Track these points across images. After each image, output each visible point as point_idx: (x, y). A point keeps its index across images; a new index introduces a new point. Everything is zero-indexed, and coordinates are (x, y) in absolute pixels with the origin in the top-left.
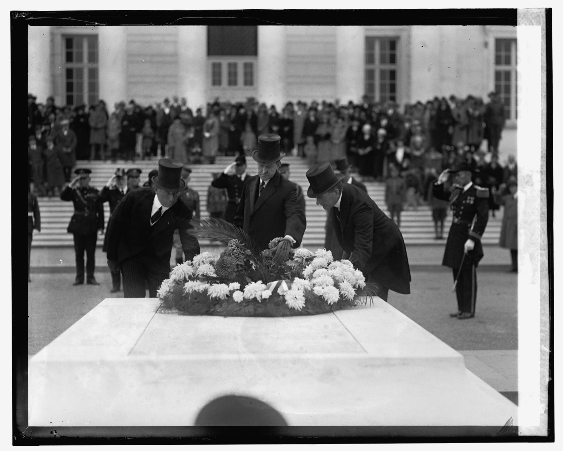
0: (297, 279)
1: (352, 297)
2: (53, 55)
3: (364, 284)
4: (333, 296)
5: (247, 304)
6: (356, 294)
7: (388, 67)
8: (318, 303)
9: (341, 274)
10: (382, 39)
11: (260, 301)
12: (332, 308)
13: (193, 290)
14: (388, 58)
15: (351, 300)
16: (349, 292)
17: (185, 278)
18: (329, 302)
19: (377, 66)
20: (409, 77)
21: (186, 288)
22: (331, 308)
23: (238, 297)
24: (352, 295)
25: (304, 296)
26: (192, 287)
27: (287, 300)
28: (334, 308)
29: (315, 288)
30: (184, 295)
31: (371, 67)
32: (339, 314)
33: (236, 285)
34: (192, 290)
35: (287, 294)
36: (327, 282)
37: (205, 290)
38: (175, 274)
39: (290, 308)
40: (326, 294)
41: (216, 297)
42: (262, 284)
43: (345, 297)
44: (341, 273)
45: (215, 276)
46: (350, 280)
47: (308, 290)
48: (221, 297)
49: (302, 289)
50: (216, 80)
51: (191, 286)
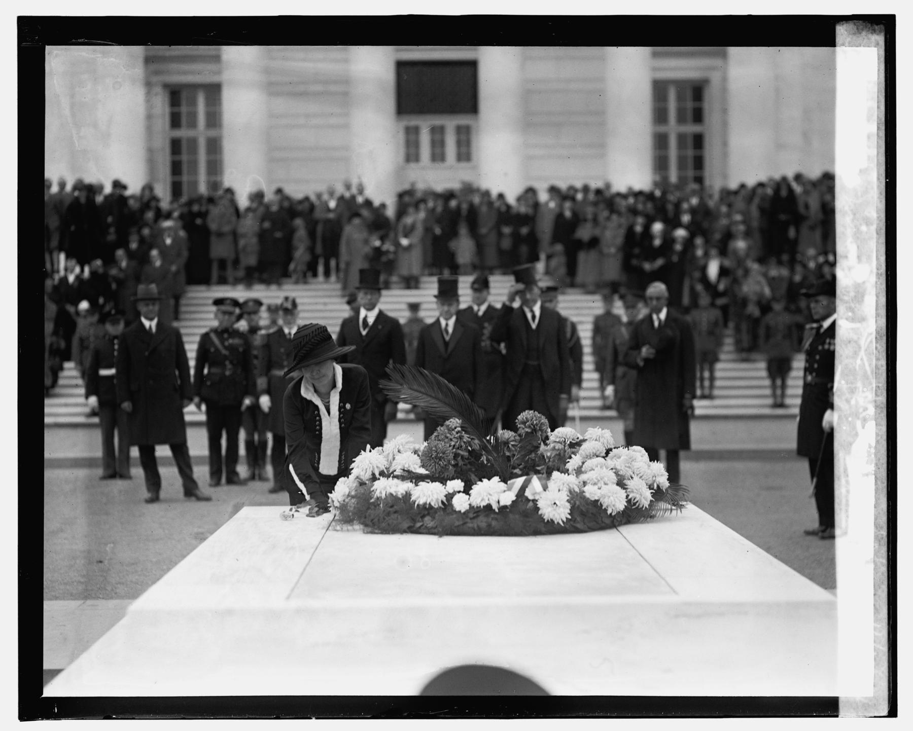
0: (556, 474)
1: (646, 503)
2: (149, 117)
3: (667, 484)
4: (615, 501)
5: (475, 515)
6: (654, 500)
7: (691, 129)
8: (592, 514)
9: (629, 467)
10: (680, 84)
11: (497, 510)
12: (615, 521)
13: (387, 493)
14: (690, 115)
15: (644, 509)
16: (641, 495)
17: (373, 474)
18: (609, 512)
19: (673, 128)
20: (725, 144)
21: (376, 490)
22: (613, 522)
23: (461, 503)
24: (646, 500)
25: (568, 501)
26: (385, 488)
27: (541, 507)
28: (617, 520)
29: (586, 489)
30: (372, 501)
31: (662, 129)
32: (626, 530)
33: (457, 485)
34: (386, 492)
35: (541, 498)
36: (606, 479)
37: (406, 492)
38: (358, 467)
39: (546, 521)
40: (605, 498)
41: (425, 504)
42: (499, 482)
43: (635, 504)
44: (627, 465)
45: (423, 471)
46: (643, 476)
47: (574, 491)
48: (433, 504)
49: (565, 489)
50: (411, 155)
51: (384, 488)
